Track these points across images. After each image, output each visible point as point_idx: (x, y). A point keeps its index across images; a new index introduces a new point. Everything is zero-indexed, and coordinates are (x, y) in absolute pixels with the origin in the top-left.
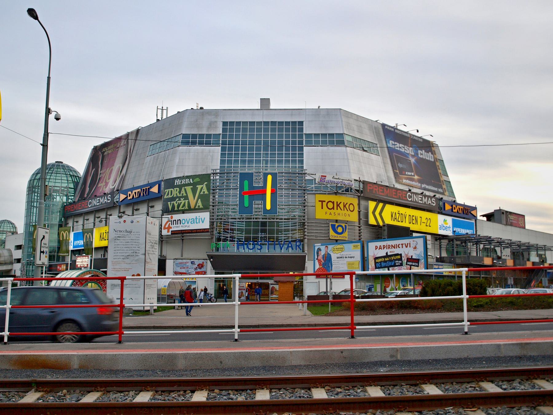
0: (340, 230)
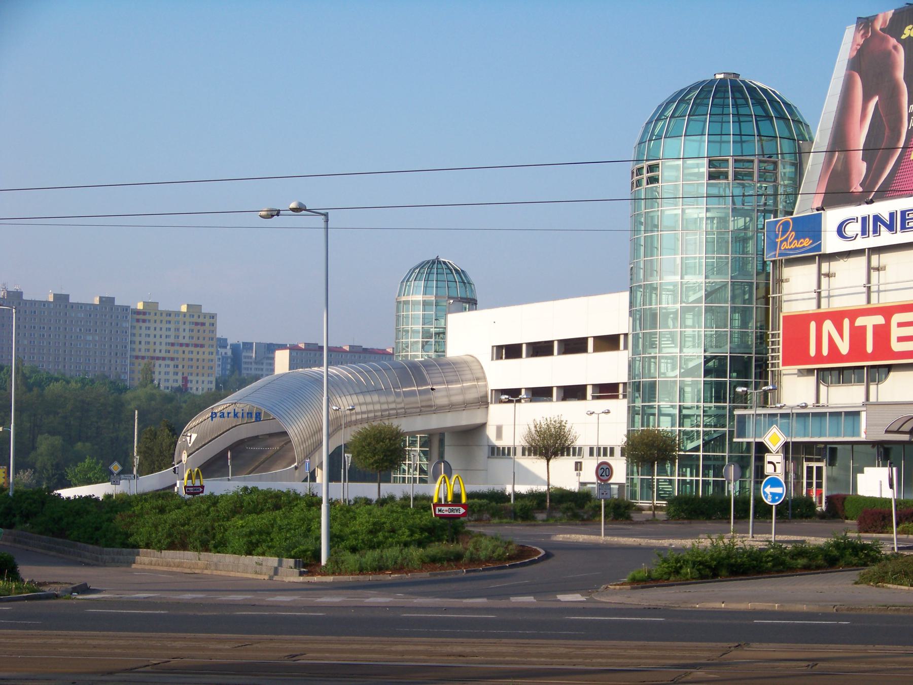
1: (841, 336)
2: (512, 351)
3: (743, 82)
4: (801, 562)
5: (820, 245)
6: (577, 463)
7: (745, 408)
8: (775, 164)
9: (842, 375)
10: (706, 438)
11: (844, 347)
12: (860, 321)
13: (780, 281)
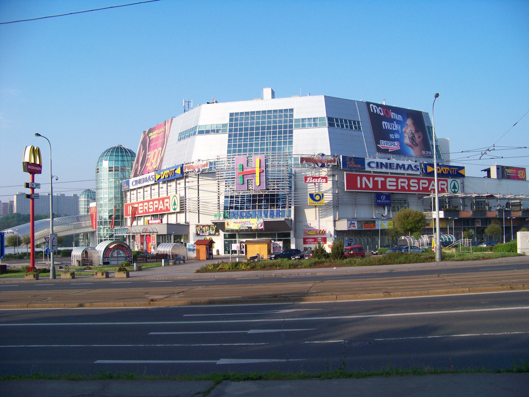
0: (317, 198)
3: (123, 147)
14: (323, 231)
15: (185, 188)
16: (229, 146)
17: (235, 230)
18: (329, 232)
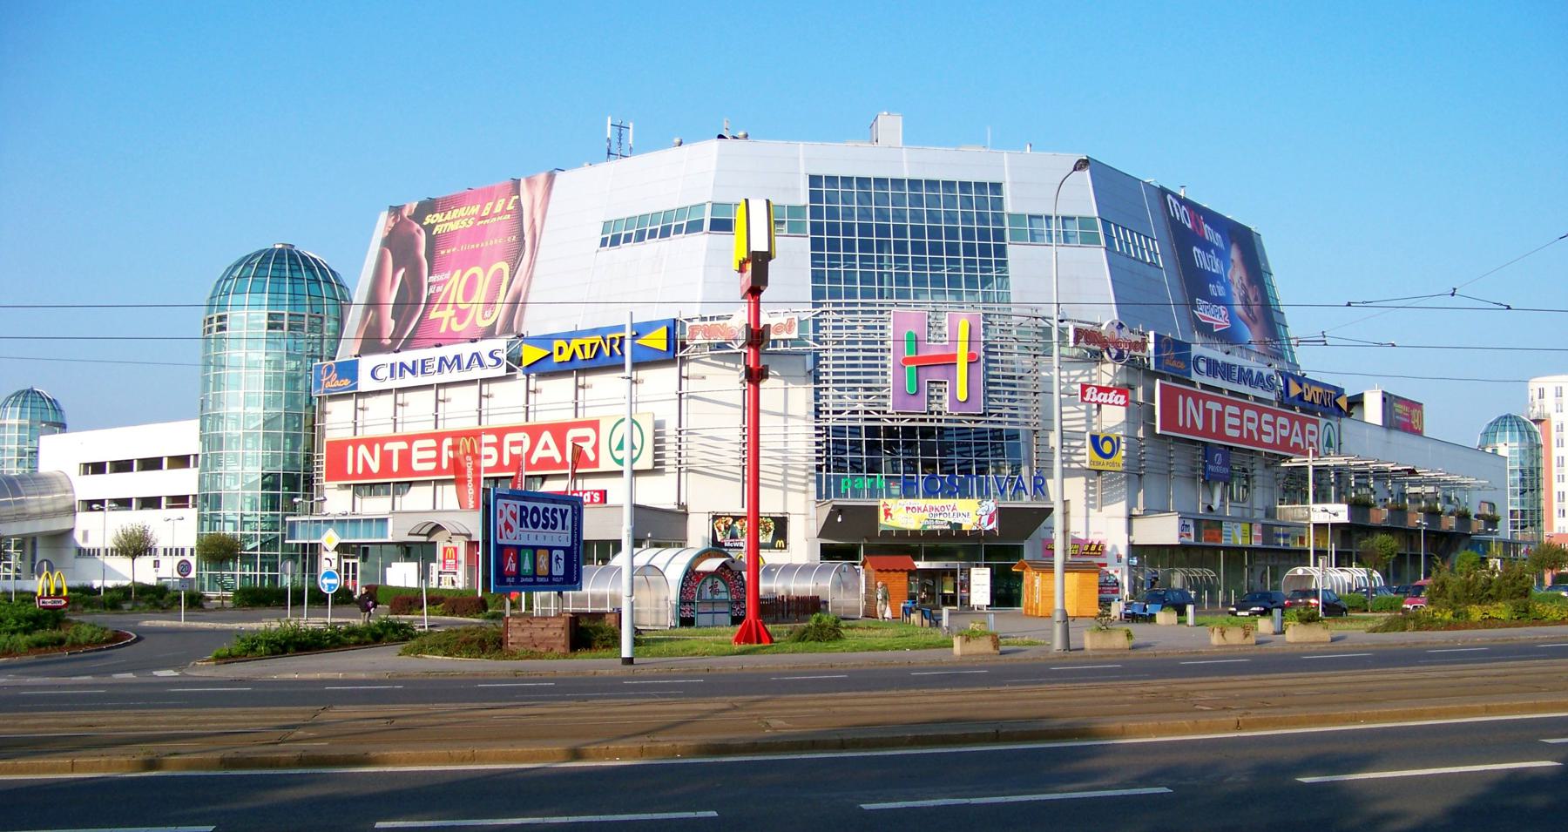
0: (1107, 448)
1: (373, 457)
2: (98, 468)
3: (298, 252)
4: (353, 639)
5: (357, 384)
6: (155, 561)
7: (295, 515)
8: (322, 318)
9: (374, 490)
10: (263, 540)
11: (375, 466)
12: (388, 446)
13: (323, 413)
14: (1098, 546)
15: (680, 395)
16: (817, 277)
17: (911, 531)
18: (1114, 547)
